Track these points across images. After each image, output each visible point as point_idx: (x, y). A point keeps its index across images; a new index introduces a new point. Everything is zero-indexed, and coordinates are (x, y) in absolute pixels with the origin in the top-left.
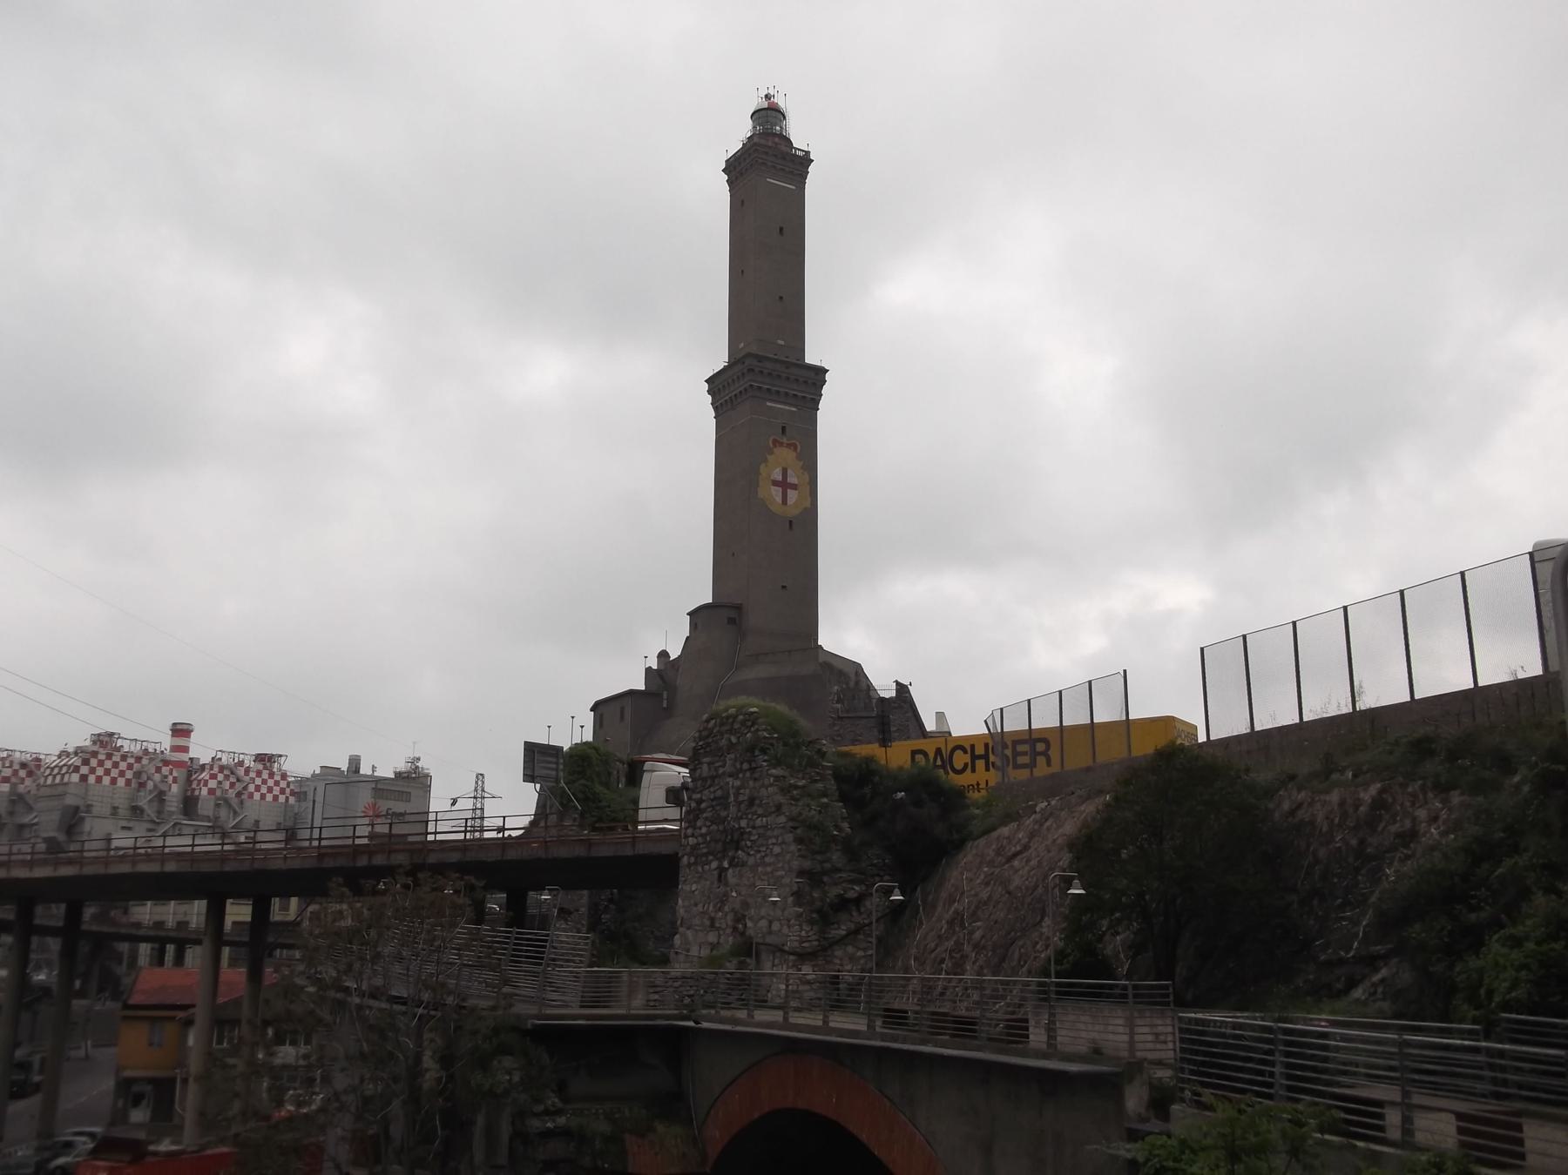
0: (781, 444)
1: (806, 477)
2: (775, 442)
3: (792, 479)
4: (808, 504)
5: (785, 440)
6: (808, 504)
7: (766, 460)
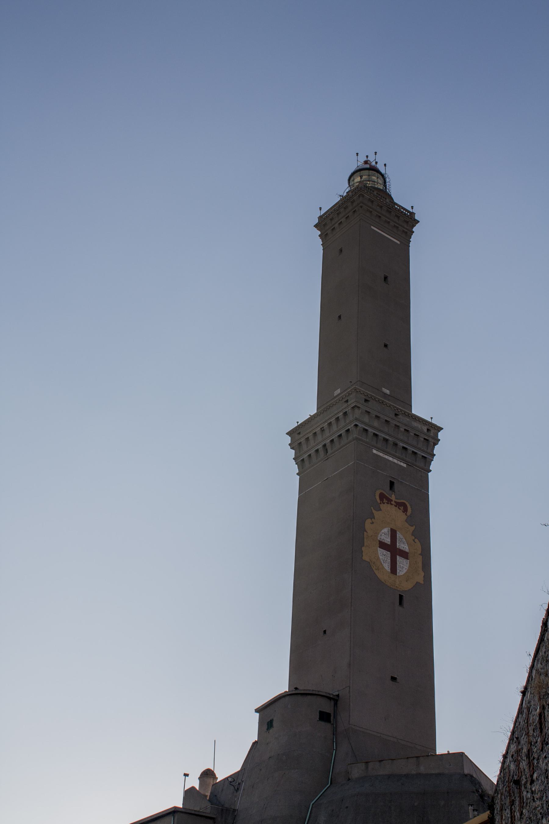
0: (389, 501)
2: (382, 496)
3: (402, 545)
4: (420, 578)
5: (393, 498)
6: (420, 578)
7: (372, 517)
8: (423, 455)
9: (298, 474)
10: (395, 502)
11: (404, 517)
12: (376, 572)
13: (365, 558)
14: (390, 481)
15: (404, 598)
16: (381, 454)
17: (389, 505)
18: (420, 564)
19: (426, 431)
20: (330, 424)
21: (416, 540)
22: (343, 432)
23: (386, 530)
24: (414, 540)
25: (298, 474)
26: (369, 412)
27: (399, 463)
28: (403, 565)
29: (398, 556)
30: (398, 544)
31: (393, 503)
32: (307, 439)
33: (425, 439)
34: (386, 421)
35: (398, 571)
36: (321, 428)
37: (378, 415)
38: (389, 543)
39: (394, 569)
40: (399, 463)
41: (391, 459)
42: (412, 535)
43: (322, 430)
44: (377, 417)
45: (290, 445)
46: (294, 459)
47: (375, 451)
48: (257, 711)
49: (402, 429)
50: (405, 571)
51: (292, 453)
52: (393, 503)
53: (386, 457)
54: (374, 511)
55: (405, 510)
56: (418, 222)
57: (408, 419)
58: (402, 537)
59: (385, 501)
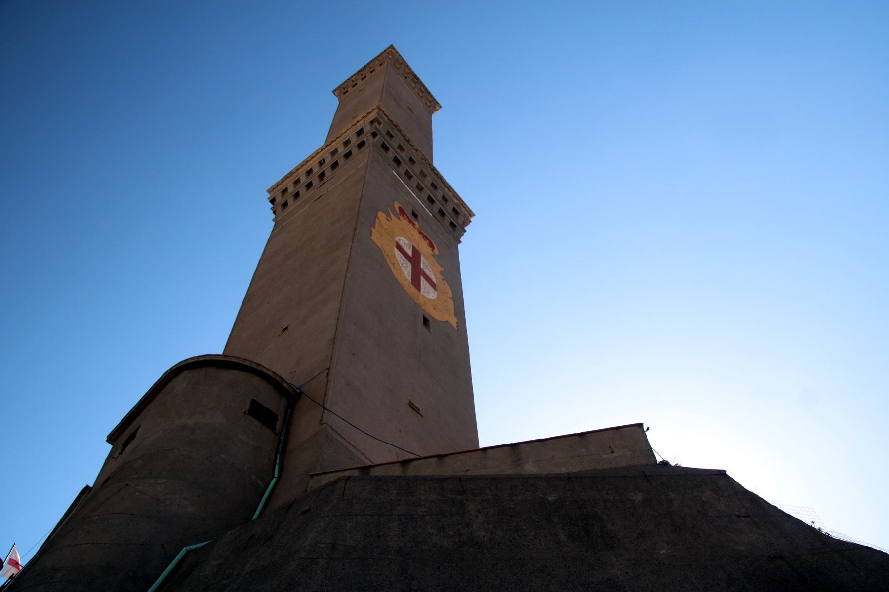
4: (453, 321)
5: (416, 223)
12: (391, 267)
23: (407, 242)
28: (428, 293)
29: (422, 278)
35: (422, 290)
39: (416, 283)
42: (441, 273)
48: (111, 439)
55: (431, 245)
56: (440, 107)
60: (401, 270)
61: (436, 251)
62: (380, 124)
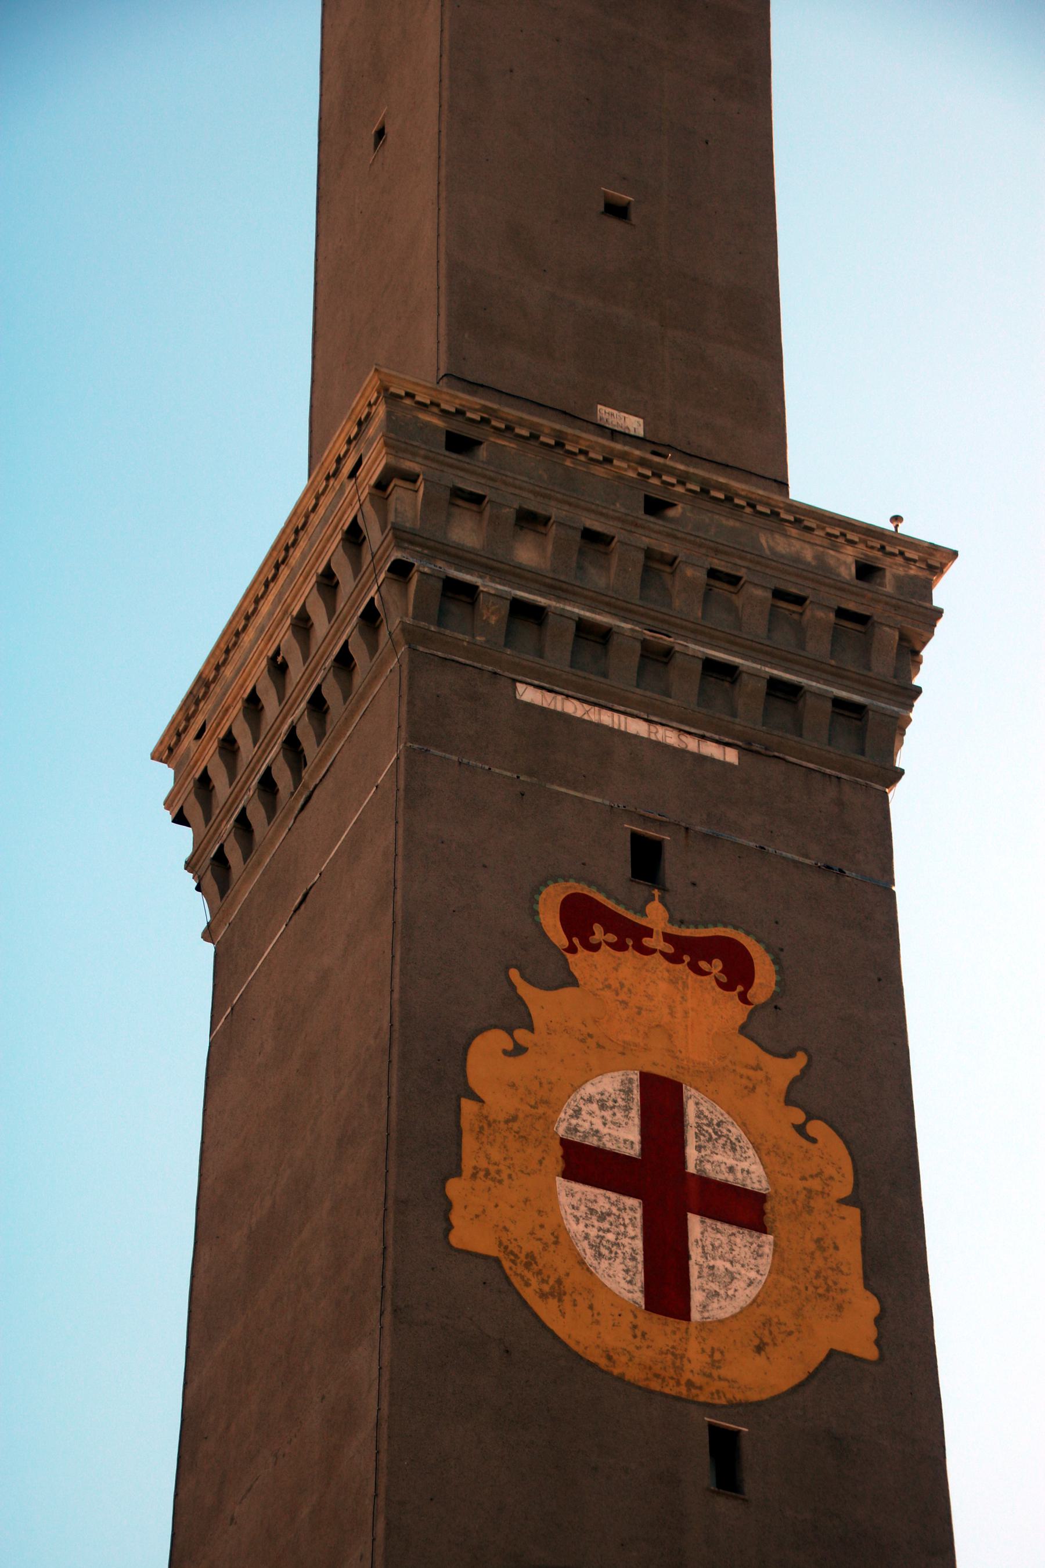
0: (631, 936)
1: (832, 1157)
2: (579, 916)
4: (854, 1329)
5: (656, 916)
6: (854, 1329)
8: (844, 694)
9: (208, 934)
10: (668, 938)
11: (731, 1011)
12: (547, 1311)
13: (468, 1234)
14: (635, 836)
15: (746, 1446)
16: (573, 708)
17: (630, 956)
18: (851, 1254)
19: (848, 572)
20: (302, 624)
21: (816, 1128)
22: (350, 630)
23: (608, 1084)
24: (800, 1129)
25: (208, 934)
26: (477, 499)
27: (692, 744)
28: (728, 1268)
29: (695, 1224)
30: (692, 1154)
31: (654, 942)
32: (229, 745)
33: (842, 613)
34: (590, 536)
35: (697, 1297)
36: (273, 659)
37: (533, 505)
38: (634, 1151)
40: (692, 744)
41: (637, 727)
42: (789, 1101)
43: (278, 668)
44: (530, 520)
45: (168, 804)
46: (189, 866)
47: (528, 694)
49: (695, 574)
50: (743, 1295)
51: (183, 839)
52: (654, 942)
53: (607, 718)
54: (525, 990)
57: (731, 523)
58: (717, 1113)
59: (598, 933)
60: (593, 1285)
61: (765, 977)
62: (411, 478)
